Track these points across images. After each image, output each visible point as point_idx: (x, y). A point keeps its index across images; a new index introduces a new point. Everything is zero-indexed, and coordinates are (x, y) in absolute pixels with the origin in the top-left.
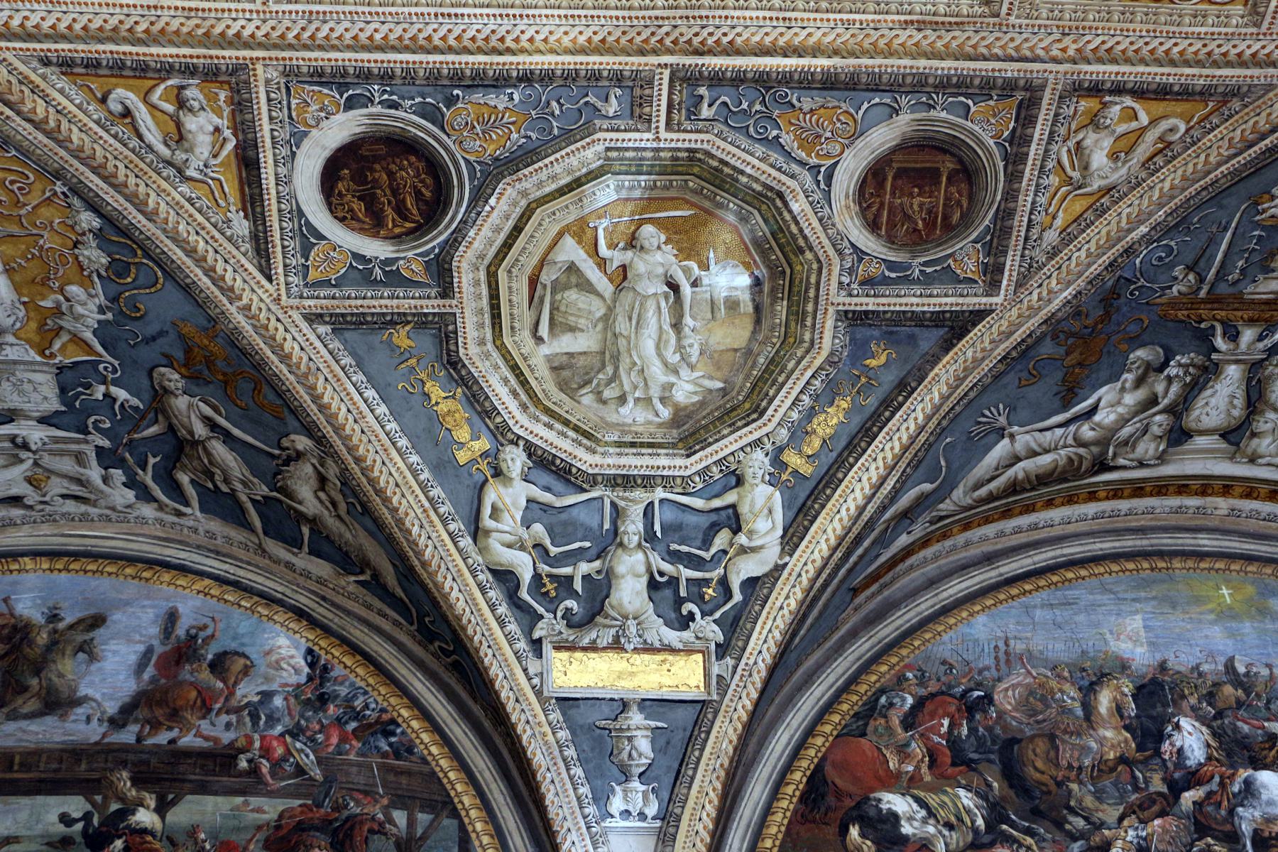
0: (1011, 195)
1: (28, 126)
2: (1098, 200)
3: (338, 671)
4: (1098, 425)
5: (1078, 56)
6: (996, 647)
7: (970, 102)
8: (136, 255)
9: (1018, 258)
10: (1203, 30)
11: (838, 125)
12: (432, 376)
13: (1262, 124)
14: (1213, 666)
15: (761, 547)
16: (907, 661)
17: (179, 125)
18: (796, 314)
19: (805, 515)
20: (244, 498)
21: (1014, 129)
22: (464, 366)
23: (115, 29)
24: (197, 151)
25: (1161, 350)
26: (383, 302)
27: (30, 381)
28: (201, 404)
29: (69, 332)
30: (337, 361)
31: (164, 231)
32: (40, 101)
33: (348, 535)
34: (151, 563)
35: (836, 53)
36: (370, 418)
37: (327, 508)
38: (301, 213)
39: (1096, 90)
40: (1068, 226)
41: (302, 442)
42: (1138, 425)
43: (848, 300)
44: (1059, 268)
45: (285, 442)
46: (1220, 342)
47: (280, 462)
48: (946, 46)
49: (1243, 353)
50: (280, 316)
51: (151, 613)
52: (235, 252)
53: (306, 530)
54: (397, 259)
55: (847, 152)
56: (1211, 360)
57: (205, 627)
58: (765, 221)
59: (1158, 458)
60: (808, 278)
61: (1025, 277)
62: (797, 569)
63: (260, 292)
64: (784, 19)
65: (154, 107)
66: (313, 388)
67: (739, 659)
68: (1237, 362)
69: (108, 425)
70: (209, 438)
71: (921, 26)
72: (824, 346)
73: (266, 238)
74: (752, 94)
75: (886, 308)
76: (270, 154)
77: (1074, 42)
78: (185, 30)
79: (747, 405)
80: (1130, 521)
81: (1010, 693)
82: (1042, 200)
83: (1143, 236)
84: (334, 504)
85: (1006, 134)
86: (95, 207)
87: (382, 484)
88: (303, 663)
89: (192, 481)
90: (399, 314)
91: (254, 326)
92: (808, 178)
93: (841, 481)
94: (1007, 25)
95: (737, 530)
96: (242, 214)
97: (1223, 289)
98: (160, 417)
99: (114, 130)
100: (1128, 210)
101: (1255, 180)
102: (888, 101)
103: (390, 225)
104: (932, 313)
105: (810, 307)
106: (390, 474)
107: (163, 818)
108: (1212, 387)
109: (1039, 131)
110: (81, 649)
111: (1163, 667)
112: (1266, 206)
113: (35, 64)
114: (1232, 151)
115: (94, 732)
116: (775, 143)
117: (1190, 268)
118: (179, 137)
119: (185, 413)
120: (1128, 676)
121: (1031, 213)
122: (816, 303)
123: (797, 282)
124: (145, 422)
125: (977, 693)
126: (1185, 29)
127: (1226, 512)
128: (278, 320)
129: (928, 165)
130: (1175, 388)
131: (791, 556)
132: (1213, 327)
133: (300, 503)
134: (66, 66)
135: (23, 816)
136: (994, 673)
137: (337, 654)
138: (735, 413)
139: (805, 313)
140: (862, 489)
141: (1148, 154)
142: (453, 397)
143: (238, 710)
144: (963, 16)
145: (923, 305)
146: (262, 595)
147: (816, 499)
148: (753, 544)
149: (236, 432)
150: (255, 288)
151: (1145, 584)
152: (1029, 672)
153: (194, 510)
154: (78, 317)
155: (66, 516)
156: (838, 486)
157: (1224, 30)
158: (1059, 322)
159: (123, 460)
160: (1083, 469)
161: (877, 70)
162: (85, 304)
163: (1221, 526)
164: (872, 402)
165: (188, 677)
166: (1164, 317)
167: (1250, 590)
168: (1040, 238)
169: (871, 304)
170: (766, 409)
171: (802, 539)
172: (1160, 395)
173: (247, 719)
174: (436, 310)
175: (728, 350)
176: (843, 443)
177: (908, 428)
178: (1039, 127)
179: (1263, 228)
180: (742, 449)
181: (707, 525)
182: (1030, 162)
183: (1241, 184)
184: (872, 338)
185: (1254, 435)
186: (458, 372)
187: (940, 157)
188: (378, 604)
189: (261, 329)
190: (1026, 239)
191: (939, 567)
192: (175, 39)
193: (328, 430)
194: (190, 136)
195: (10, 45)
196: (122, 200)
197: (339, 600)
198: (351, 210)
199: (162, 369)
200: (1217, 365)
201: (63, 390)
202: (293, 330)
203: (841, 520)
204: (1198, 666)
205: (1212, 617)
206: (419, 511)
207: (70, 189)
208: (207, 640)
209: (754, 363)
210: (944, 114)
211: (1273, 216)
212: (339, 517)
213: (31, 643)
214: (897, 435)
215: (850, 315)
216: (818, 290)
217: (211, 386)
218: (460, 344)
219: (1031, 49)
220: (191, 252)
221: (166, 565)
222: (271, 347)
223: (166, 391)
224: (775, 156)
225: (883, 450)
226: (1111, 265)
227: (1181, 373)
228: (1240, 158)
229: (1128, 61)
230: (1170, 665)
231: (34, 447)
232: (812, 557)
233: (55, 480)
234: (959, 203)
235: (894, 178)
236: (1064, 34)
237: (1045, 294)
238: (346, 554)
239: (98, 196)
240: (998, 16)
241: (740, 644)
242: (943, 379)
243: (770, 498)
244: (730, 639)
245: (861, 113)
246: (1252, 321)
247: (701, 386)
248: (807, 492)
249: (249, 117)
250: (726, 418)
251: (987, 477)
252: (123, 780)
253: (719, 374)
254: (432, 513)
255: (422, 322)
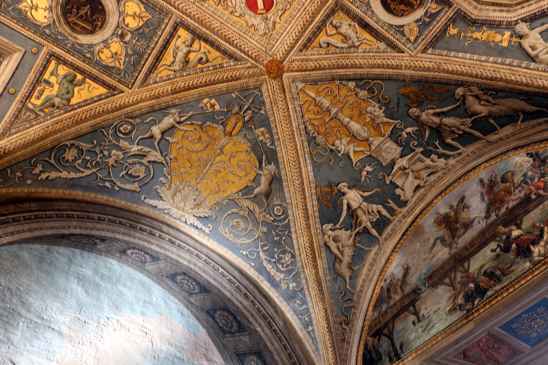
1: (314, 72)
3: (541, 151)
8: (370, 83)
12: (473, 32)
17: (341, 34)
20: (468, 130)
22: (478, 20)
23: (304, 25)
24: (352, 36)
26: (437, 26)
27: (387, 147)
28: (428, 111)
29: (381, 123)
30: (443, 55)
31: (368, 67)
32: (310, 62)
33: (503, 108)
34: (465, 174)
36: (467, 61)
37: (488, 106)
38: (391, 25)
41: (460, 91)
45: (457, 97)
47: (463, 106)
50: (416, 59)
51: (475, 185)
52: (388, 54)
53: (492, 121)
54: (427, 10)
57: (492, 175)
63: (405, 58)
65: (331, 35)
66: (444, 70)
69: (416, 143)
70: (441, 120)
73: (391, 42)
76: (367, 18)
78: (316, 7)
84: (488, 101)
86: (349, 80)
87: (490, 75)
88: (528, 158)
89: (452, 139)
90: (444, 25)
91: (413, 70)
96: (379, 42)
98: (425, 127)
99: (330, 52)
103: (415, 3)
106: (489, 70)
107: (521, 229)
110: (464, 208)
113: (300, 54)
115: (483, 224)
118: (346, 38)
119: (428, 119)
124: (423, 133)
128: (417, 61)
133: (481, 113)
134: (305, 46)
135: (481, 258)
137: (536, 147)
142: (484, 31)
143: (520, 185)
146: (501, 154)
149: (444, 110)
150: (402, 58)
153: (462, 149)
154: (378, 116)
155: (436, 181)
159: (430, 150)
162: (375, 111)
165: (498, 190)
173: (524, 185)
174: (453, 13)
186: (478, 23)
188: (534, 122)
189: (415, 68)
192: (317, 12)
193: (461, 78)
194: (346, 34)
195: (291, 54)
196: (351, 70)
197: (524, 135)
198: (401, 10)
199: (410, 111)
201: (397, 142)
202: (423, 60)
206: (508, 71)
207: (340, 80)
208: (495, 178)
212: (494, 104)
213: (450, 218)
217: (424, 102)
218: (470, 15)
220: (379, 66)
221: (470, 171)
222: (423, 71)
223: (418, 117)
231: (407, 167)
233: (422, 172)
238: (509, 116)
239: (346, 75)
249: (352, 13)
252: (501, 229)
254: (513, 68)
255: (453, 21)
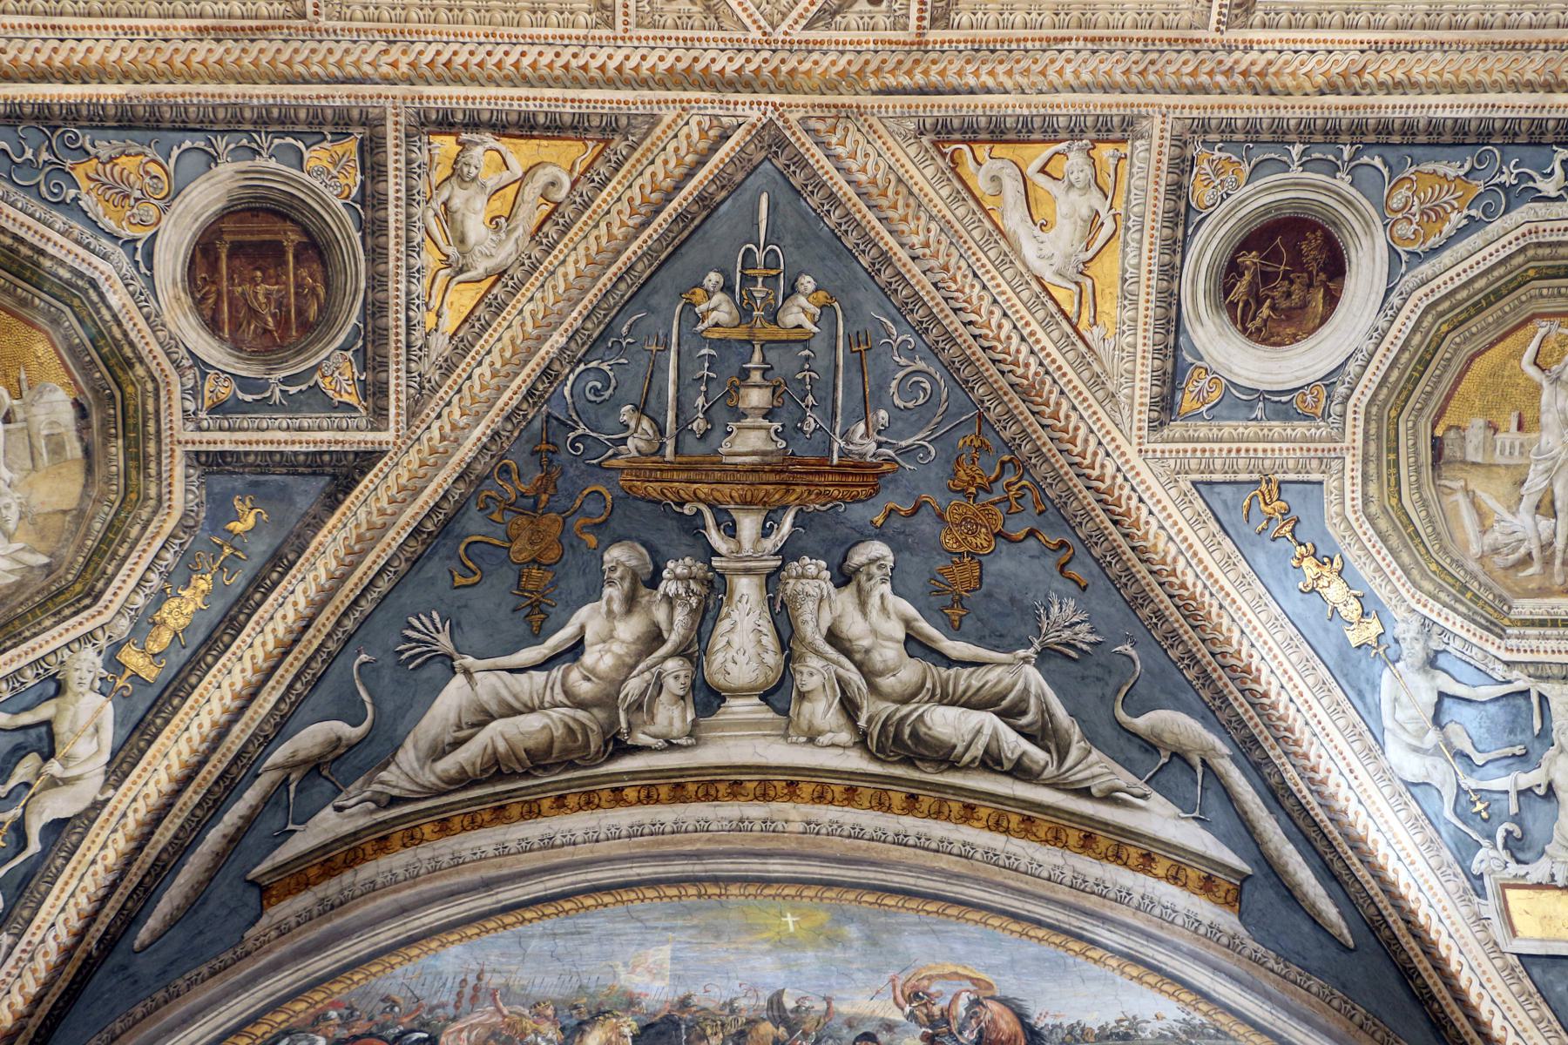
0: (377, 281)
2: (489, 291)
4: (592, 671)
5: (412, 73)
6: (464, 980)
7: (300, 145)
9: (403, 374)
10: (549, 31)
11: (147, 179)
13: (661, 176)
14: (753, 1002)
15: (78, 778)
16: (336, 997)
18: (137, 459)
19: (143, 734)
21: (363, 184)
25: (644, 551)
35: (125, 76)
39: (445, 123)
40: (459, 328)
42: (647, 675)
43: (197, 436)
44: (459, 391)
46: (715, 538)
48: (255, 63)
49: (750, 558)
55: (164, 218)
56: (712, 569)
58: (81, 322)
59: (690, 735)
60: (144, 404)
61: (417, 402)
62: (122, 807)
64: (53, 27)
67: (19, 936)
68: (747, 572)
71: (219, 35)
72: (174, 503)
74: (33, 135)
75: (248, 448)
77: (404, 52)
79: (78, 587)
80: (680, 842)
81: (464, 1035)
82: (419, 289)
83: (562, 350)
85: (355, 191)
92: (120, 254)
93: (194, 687)
94: (319, 30)
95: (47, 756)
97: (692, 447)
100: (530, 306)
101: (677, 265)
102: (201, 144)
104: (307, 454)
105: (152, 448)
108: (728, 615)
109: (393, 186)
111: (684, 1003)
112: (703, 307)
114: (637, 220)
116: (73, 208)
117: (641, 409)
120: (634, 1014)
121: (408, 309)
122: (159, 441)
123: (131, 409)
125: (417, 1035)
126: (529, 31)
127: (800, 827)
129: (267, 237)
130: (680, 615)
131: (116, 788)
132: (699, 512)
136: (451, 1011)
138: (62, 598)
139: (146, 456)
140: (221, 699)
141: (535, 222)
144: (263, 18)
145: (293, 443)
147: (159, 711)
148: (68, 774)
151: (689, 911)
152: (499, 1010)
156: (189, 694)
157: (574, 32)
158: (482, 479)
160: (593, 748)
161: (180, 100)
163: (800, 850)
164: (238, 581)
166: (628, 495)
167: (822, 917)
168: (426, 345)
169: (226, 441)
170: (102, 593)
171: (134, 766)
172: (664, 626)
175: (55, 512)
176: (200, 637)
177: (284, 617)
178: (391, 180)
179: (713, 343)
180: (67, 645)
181: (9, 747)
182: (392, 233)
183: (662, 273)
184: (234, 491)
185: (803, 696)
187: (279, 225)
190: (409, 346)
191: (420, 893)
200: (722, 576)
203: (189, 740)
204: (732, 1002)
205: (766, 946)
209: (89, 529)
210: (273, 163)
211: (717, 325)
214: (271, 626)
215: (203, 459)
216: (158, 421)
219: (356, 64)
224: (78, 228)
225: (251, 646)
226: (530, 393)
227: (682, 591)
228: (649, 231)
229: (473, 80)
230: (694, 1000)
232: (145, 790)
234: (313, 290)
235: (229, 257)
236: (389, 42)
237: (447, 429)
240: (303, 16)
241: (26, 913)
242: (330, 551)
243: (99, 711)
244: (13, 907)
245: (172, 161)
246: (747, 503)
247: (19, 562)
248: (148, 703)
250: (50, 604)
251: (448, 739)
253: (43, 546)
